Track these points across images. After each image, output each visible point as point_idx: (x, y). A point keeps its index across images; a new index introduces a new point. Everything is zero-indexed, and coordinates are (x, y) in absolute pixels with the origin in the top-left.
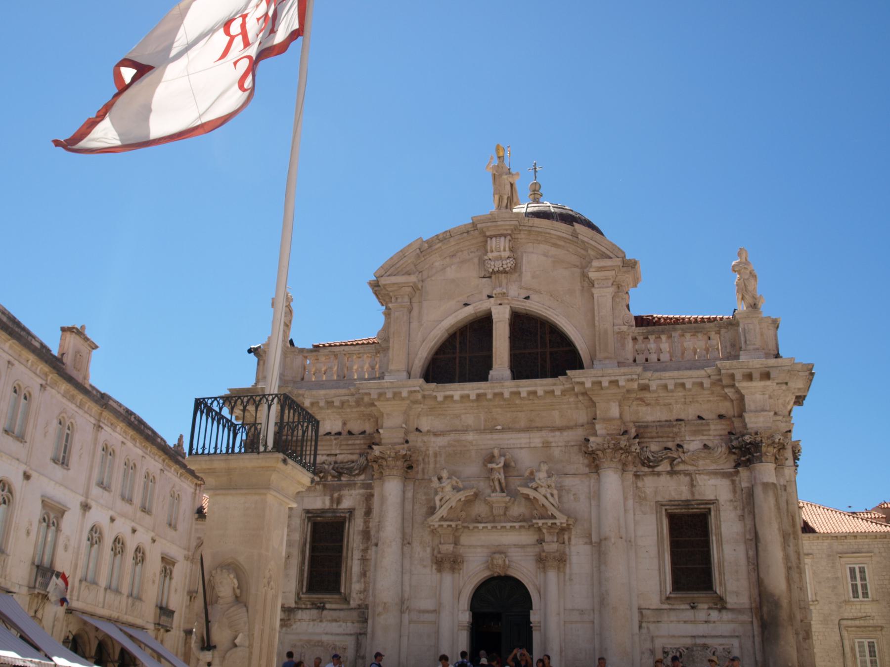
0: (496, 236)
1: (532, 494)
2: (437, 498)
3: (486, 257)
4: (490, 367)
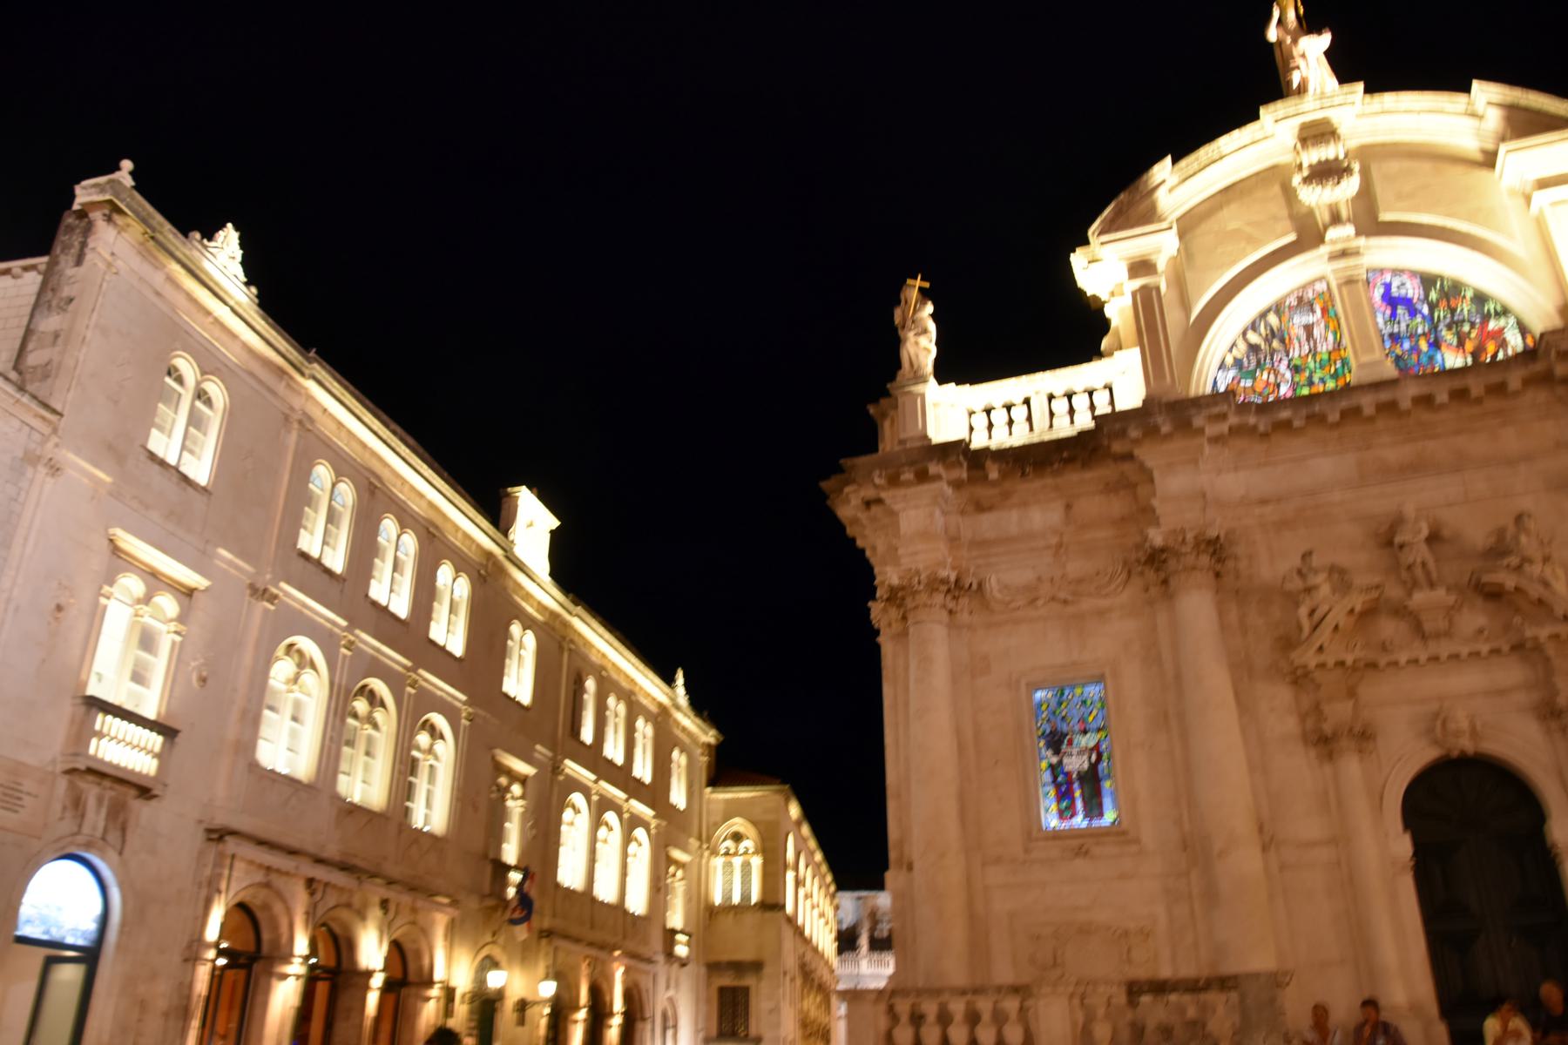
1: (1510, 581)
2: (1303, 611)
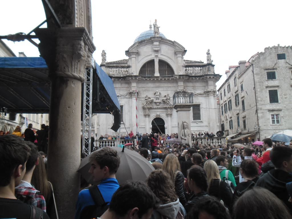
0: (156, 42)
3: (153, 47)
4: (154, 73)
